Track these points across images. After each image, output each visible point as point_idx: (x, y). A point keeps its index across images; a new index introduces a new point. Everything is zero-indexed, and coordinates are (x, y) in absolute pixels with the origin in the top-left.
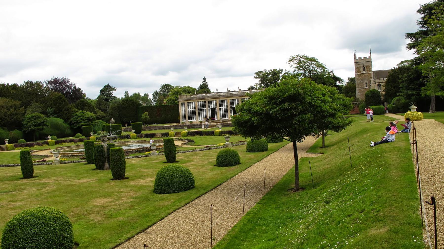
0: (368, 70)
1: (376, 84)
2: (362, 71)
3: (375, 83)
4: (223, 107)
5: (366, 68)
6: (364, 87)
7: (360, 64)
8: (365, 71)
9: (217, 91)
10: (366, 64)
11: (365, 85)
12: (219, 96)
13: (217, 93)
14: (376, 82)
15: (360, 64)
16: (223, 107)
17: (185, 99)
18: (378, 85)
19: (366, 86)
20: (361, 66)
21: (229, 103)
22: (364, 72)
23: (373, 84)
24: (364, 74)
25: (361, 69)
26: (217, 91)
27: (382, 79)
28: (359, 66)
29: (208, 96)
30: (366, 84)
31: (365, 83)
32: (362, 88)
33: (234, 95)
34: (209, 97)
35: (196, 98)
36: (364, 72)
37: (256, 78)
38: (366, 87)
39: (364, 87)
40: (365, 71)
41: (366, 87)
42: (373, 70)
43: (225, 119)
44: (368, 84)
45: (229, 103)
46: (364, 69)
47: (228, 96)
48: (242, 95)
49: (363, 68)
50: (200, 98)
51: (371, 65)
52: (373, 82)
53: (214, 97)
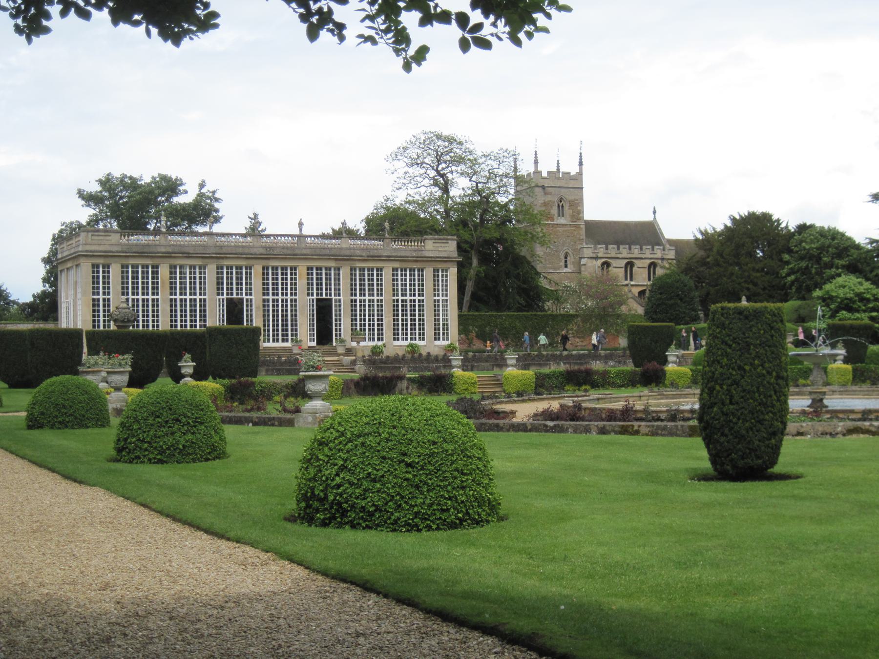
0: (573, 216)
1: (600, 262)
2: (556, 215)
3: (597, 258)
4: (280, 297)
5: (566, 208)
6: (561, 266)
7: (550, 194)
8: (563, 216)
9: (301, 230)
10: (569, 196)
11: (563, 263)
12: (265, 248)
13: (300, 236)
14: (600, 255)
15: (550, 194)
16: (280, 297)
17: (115, 249)
18: (603, 264)
19: (566, 266)
20: (556, 199)
21: (301, 283)
22: (562, 221)
23: (589, 261)
24: (563, 225)
25: (554, 211)
26: (301, 230)
27: (615, 246)
28: (549, 198)
29: (221, 247)
30: (566, 257)
31: (562, 257)
32: (555, 269)
33: (324, 252)
34: (224, 250)
35: (163, 250)
36: (562, 221)
37: (89, 199)
38: (565, 270)
39: (561, 266)
40: (563, 216)
41: (565, 270)
42: (585, 218)
43: (276, 345)
44: (570, 260)
45: (301, 283)
46: (561, 213)
47: (304, 252)
48: (358, 252)
49: (559, 206)
50: (186, 250)
51: (582, 199)
52: (592, 255)
53: (246, 251)
